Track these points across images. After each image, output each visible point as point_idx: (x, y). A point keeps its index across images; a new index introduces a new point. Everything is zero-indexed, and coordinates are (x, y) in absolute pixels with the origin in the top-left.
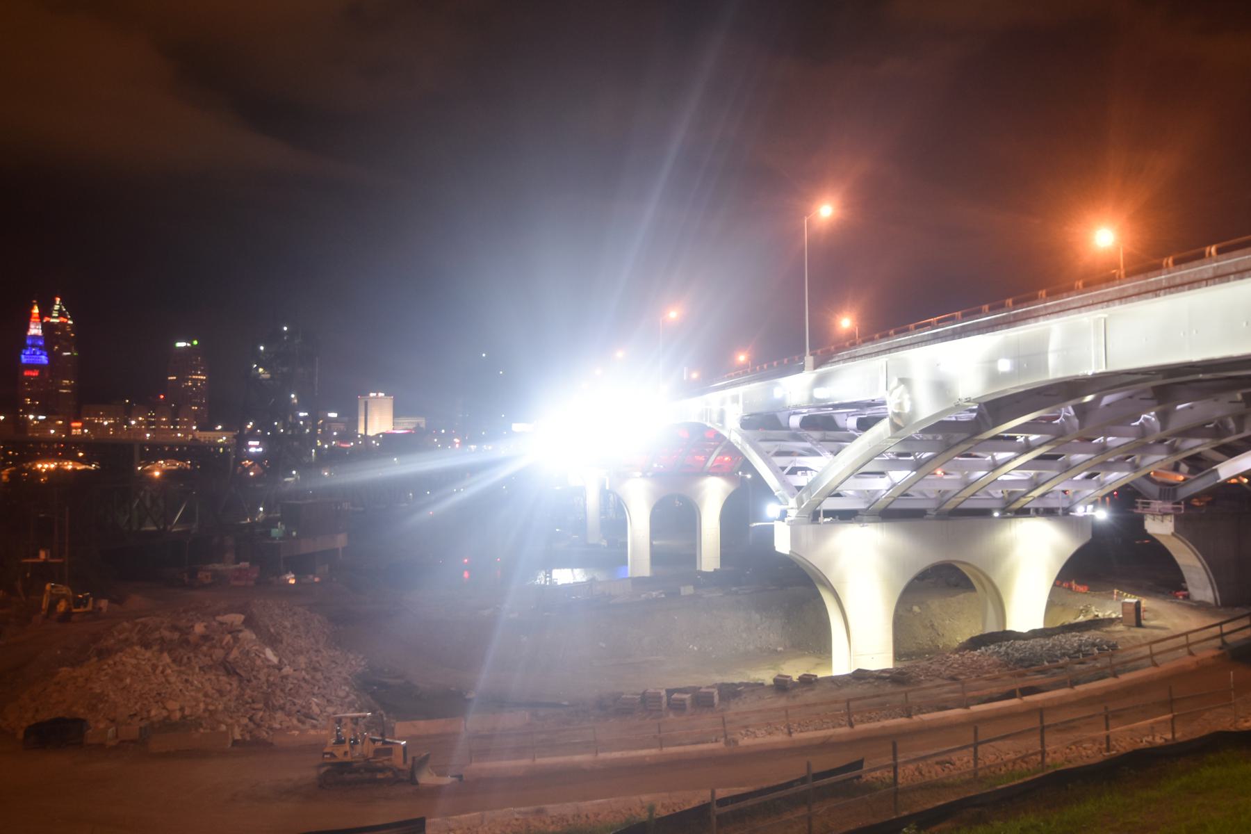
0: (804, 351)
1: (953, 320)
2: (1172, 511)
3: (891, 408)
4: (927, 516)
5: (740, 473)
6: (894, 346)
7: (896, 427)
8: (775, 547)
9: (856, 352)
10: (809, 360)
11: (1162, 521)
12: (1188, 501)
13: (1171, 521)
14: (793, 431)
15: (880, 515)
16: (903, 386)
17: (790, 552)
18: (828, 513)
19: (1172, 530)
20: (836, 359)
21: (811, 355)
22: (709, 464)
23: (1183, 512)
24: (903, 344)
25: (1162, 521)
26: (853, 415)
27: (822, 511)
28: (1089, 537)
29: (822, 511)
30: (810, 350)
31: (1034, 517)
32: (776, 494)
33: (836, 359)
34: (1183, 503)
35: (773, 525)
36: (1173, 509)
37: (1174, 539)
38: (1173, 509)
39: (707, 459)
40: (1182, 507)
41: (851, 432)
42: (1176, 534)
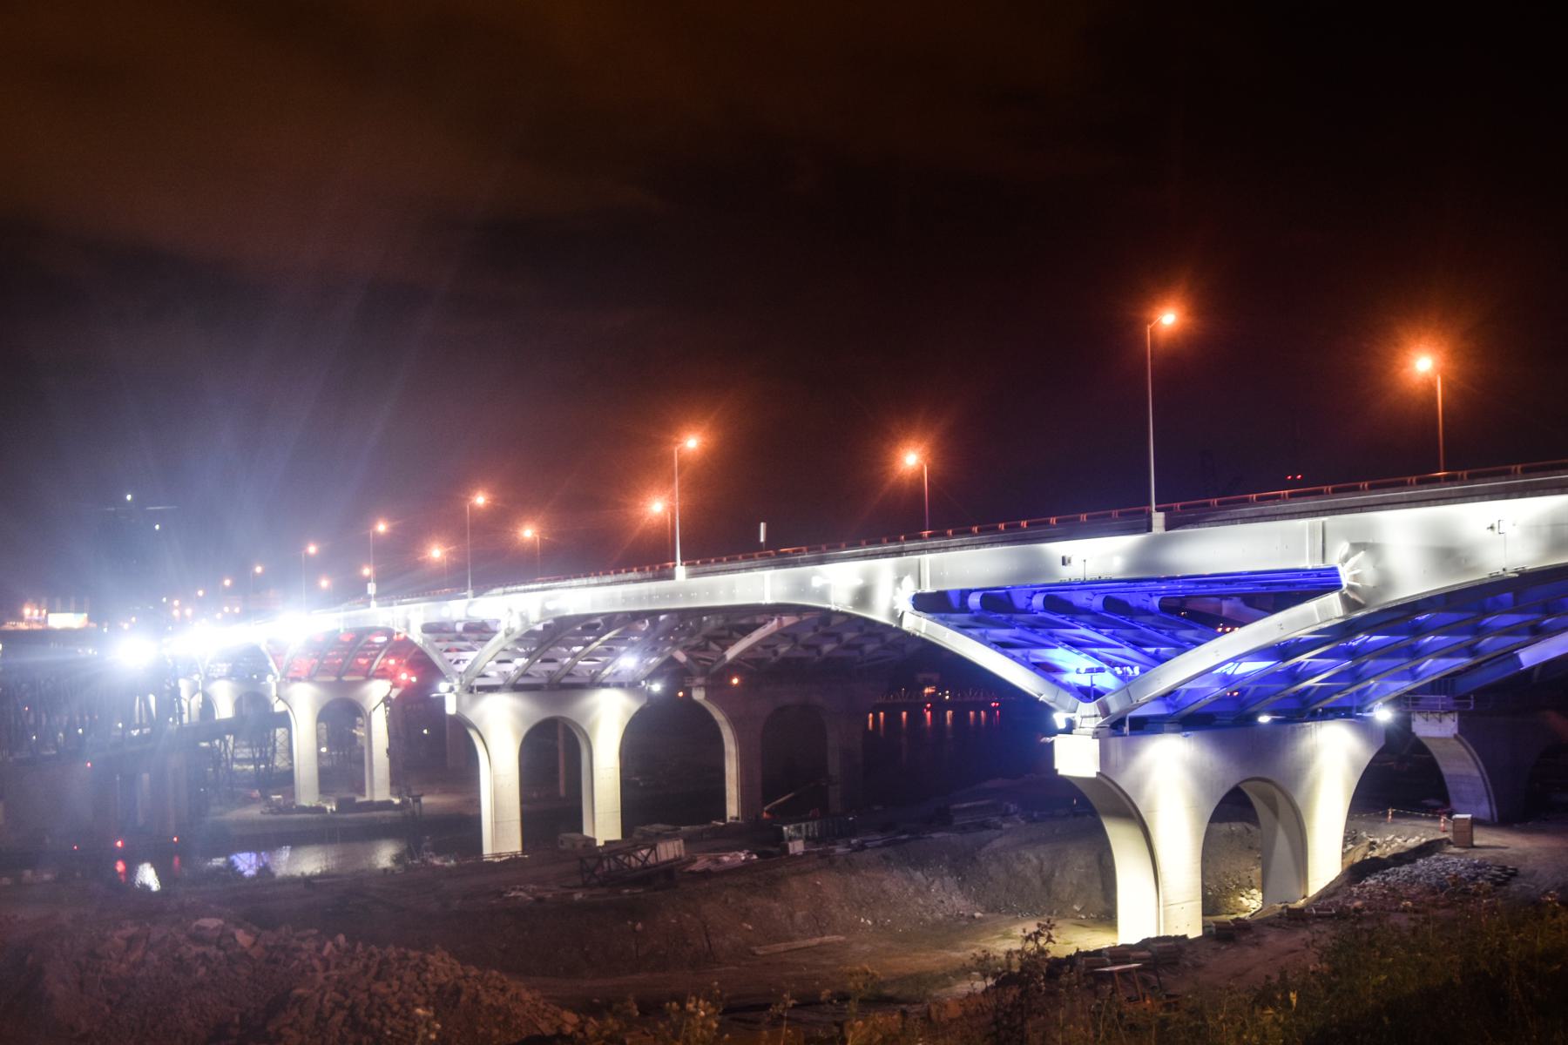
0: (1149, 504)
1: (1507, 474)
2: (1456, 708)
3: (1346, 580)
4: (1217, 722)
5: (643, 683)
6: (1372, 503)
7: (1350, 604)
8: (1056, 771)
9: (1278, 509)
10: (1158, 519)
11: (1440, 721)
12: (1483, 693)
13: (1454, 721)
14: (976, 614)
15: (1180, 723)
16: (1362, 553)
17: (1098, 773)
18: (1133, 720)
19: (1456, 731)
20: (1220, 518)
21: (1158, 510)
22: (607, 672)
23: (1472, 708)
24: (1391, 500)
25: (1440, 721)
26: (1041, 592)
27: (1128, 718)
28: (1383, 743)
29: (1128, 718)
30: (1156, 504)
31: (1331, 719)
32: (1041, 699)
33: (1220, 518)
34: (1472, 697)
35: (1052, 743)
36: (1455, 705)
37: (1456, 742)
38: (1455, 705)
39: (605, 665)
40: (1472, 702)
41: (1040, 614)
42: (1459, 736)
